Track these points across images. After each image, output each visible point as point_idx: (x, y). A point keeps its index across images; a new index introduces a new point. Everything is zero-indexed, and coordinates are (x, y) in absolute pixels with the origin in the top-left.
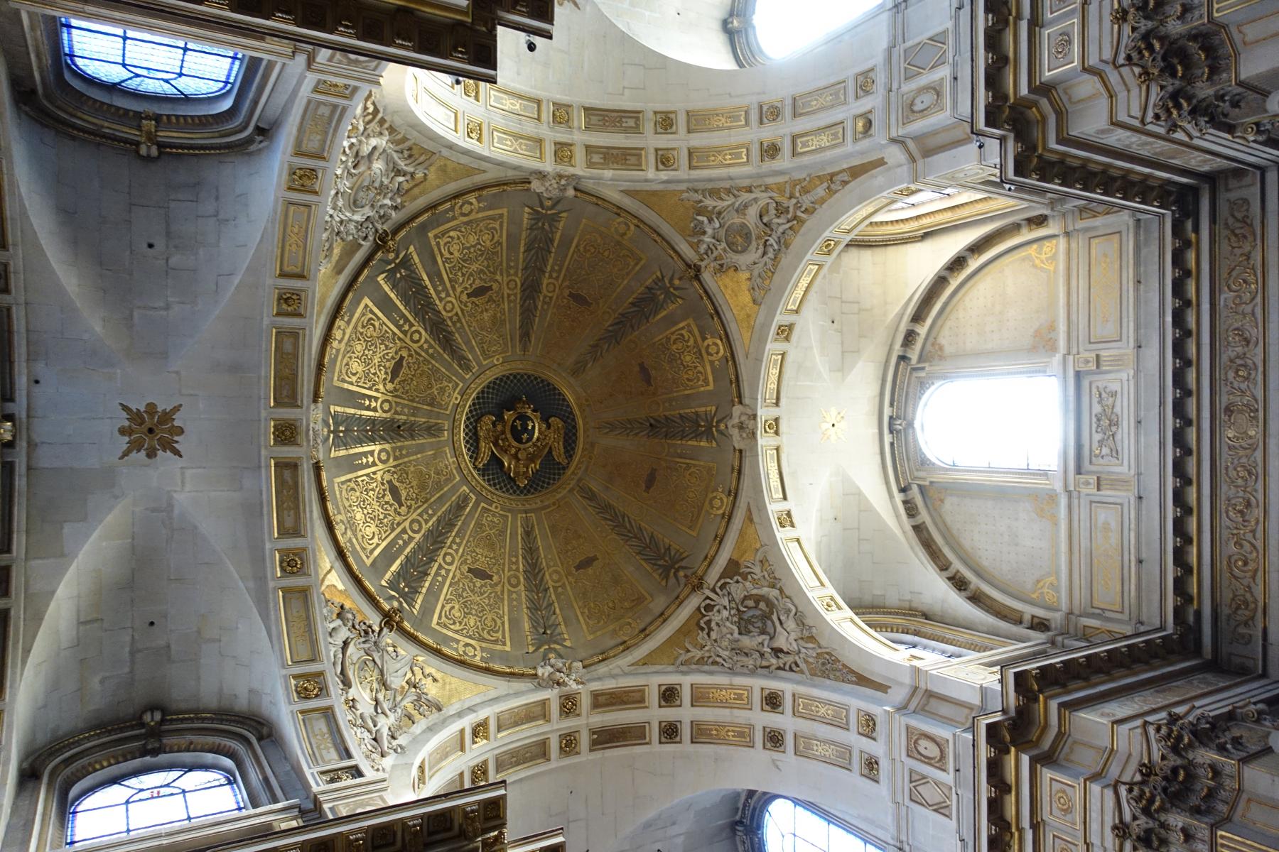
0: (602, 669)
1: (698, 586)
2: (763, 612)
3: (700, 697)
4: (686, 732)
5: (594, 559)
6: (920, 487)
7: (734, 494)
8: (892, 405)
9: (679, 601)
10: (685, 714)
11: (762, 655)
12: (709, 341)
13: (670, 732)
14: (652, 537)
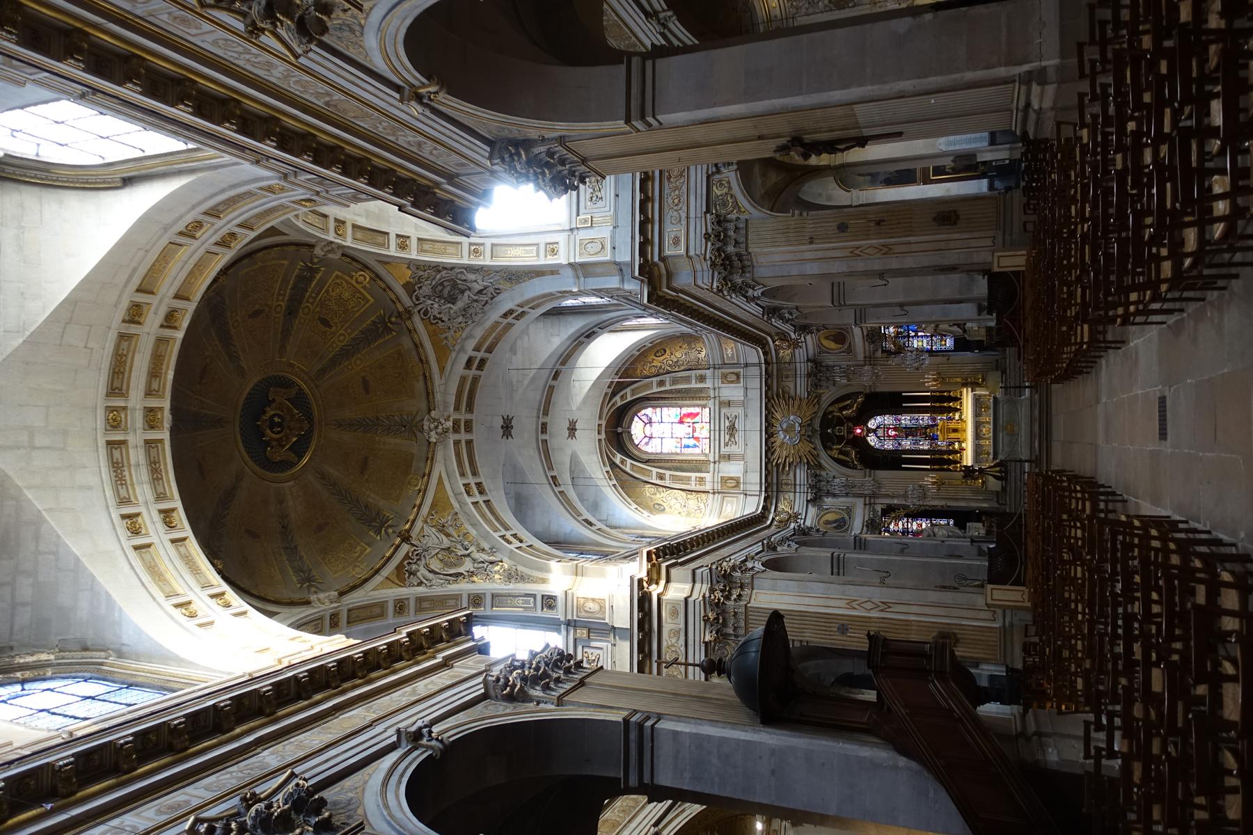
0: (438, 397)
1: (409, 312)
5: (364, 378)
7: (366, 267)
9: (411, 331)
11: (476, 301)
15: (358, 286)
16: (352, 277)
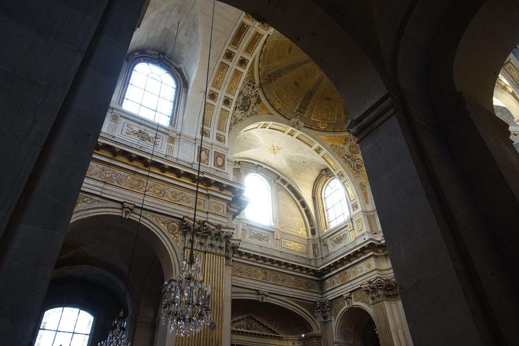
2: (247, 108)
3: (237, 73)
4: (226, 61)
6: (239, 168)
8: (266, 168)
10: (233, 65)
12: (326, 125)
13: (229, 55)
14: (281, 76)
15: (279, 100)
16: (282, 105)
